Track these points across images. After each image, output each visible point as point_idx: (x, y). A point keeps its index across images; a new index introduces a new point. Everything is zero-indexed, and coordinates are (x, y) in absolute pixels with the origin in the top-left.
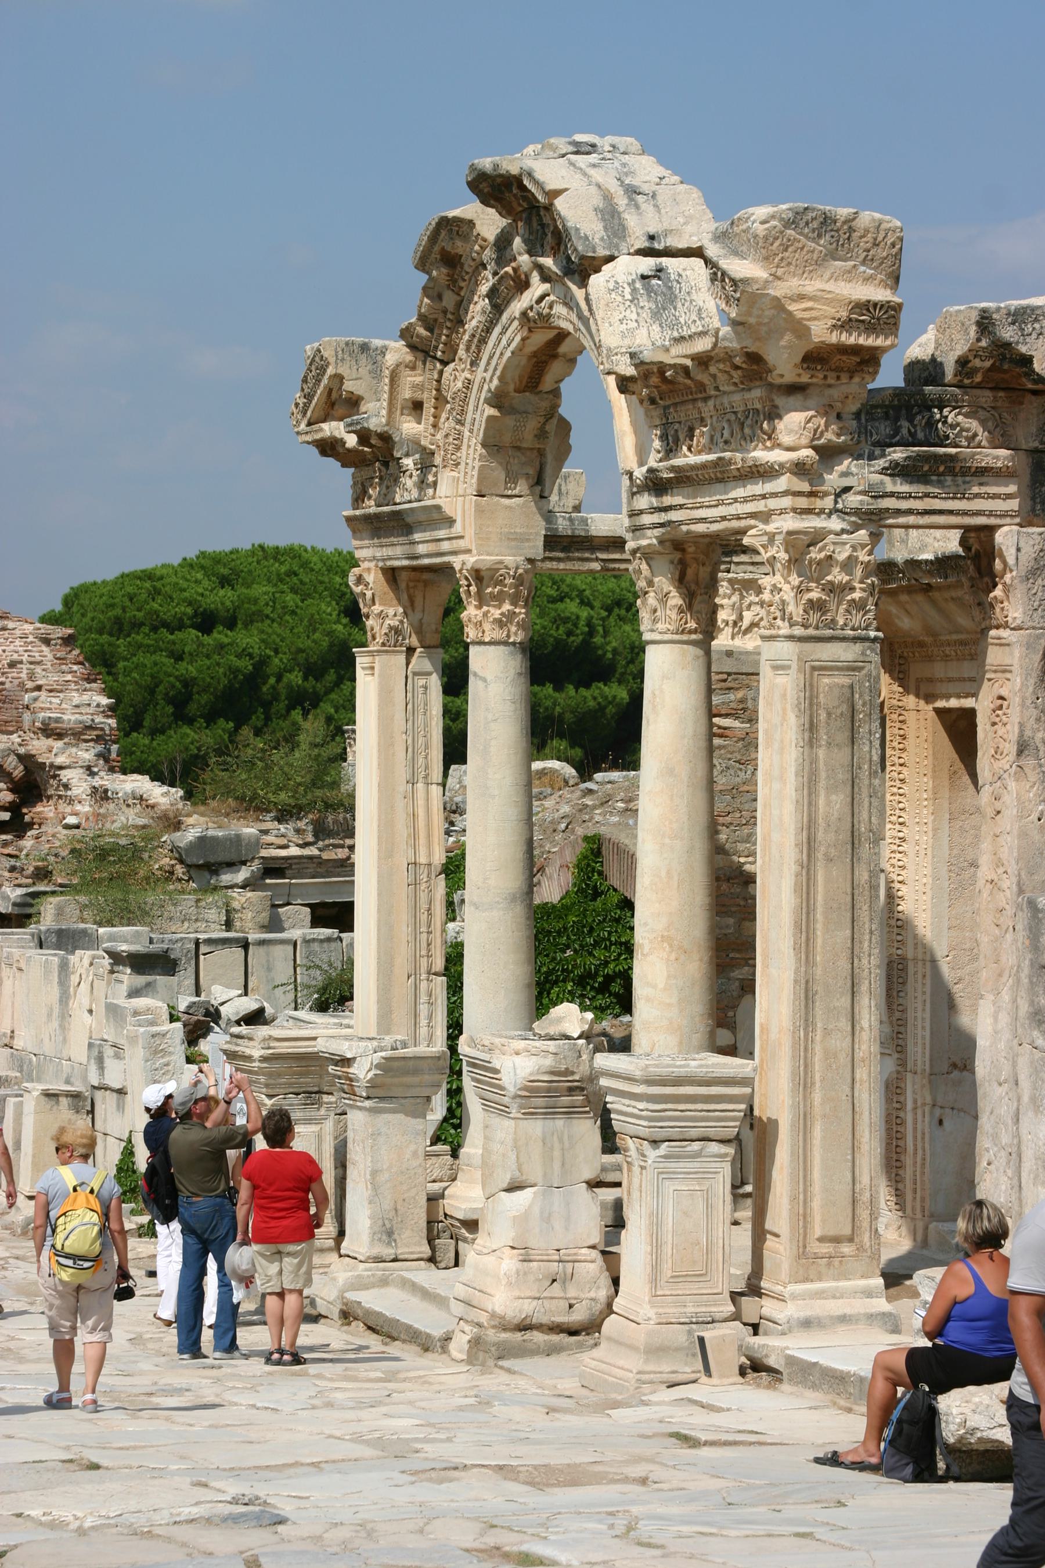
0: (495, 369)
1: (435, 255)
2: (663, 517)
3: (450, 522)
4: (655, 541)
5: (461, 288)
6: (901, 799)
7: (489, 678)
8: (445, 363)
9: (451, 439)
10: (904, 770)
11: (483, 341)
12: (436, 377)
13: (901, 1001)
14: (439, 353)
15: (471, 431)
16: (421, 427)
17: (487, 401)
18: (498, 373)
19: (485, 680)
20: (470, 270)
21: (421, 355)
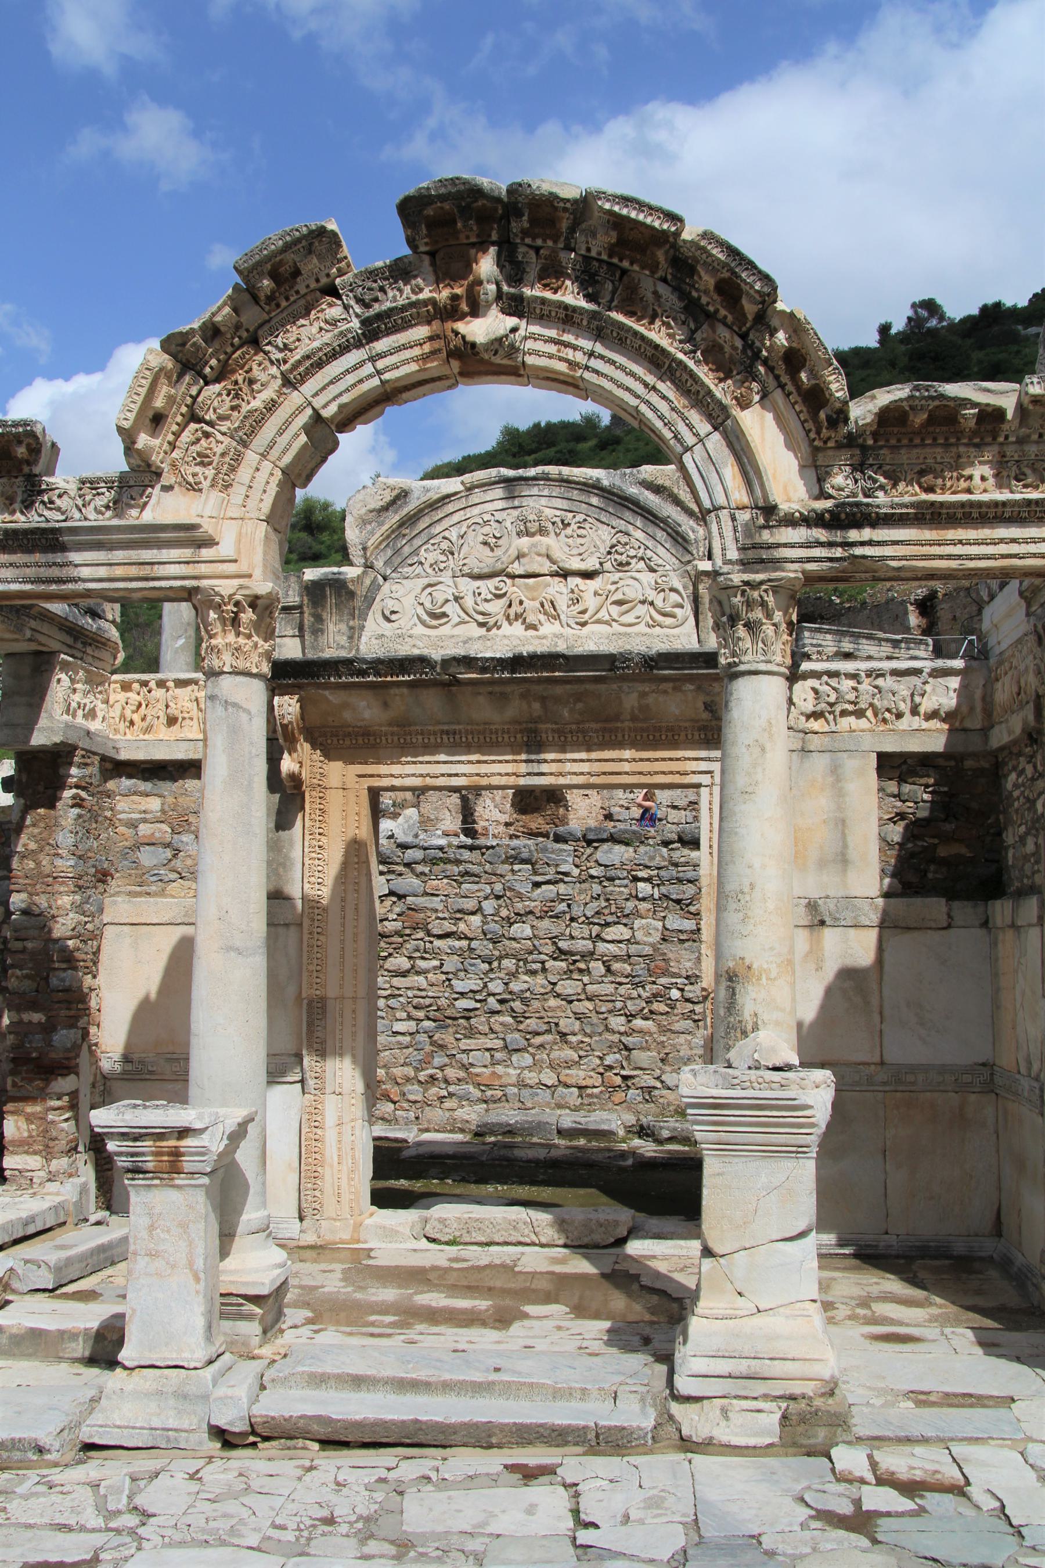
0: (340, 394)
1: (269, 266)
2: (838, 553)
3: (209, 542)
4: (800, 575)
5: (278, 306)
6: (321, 863)
7: (254, 711)
8: (207, 384)
9: (227, 459)
10: (323, 838)
11: (320, 365)
12: (194, 391)
13: (319, 1034)
14: (207, 370)
15: (264, 456)
16: (157, 442)
17: (307, 429)
18: (345, 399)
19: (249, 713)
20: (303, 291)
21: (179, 366)
